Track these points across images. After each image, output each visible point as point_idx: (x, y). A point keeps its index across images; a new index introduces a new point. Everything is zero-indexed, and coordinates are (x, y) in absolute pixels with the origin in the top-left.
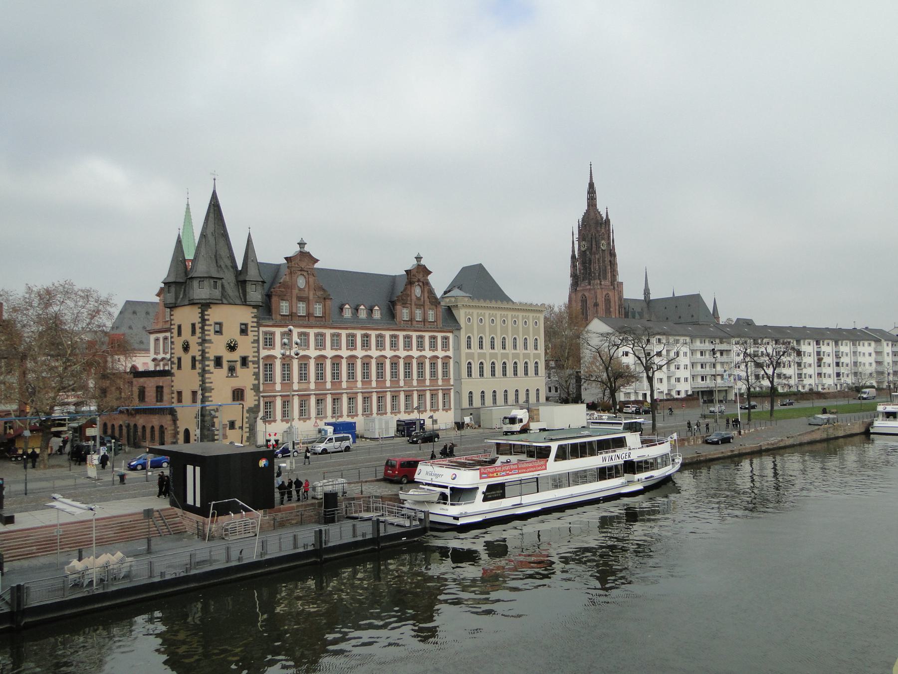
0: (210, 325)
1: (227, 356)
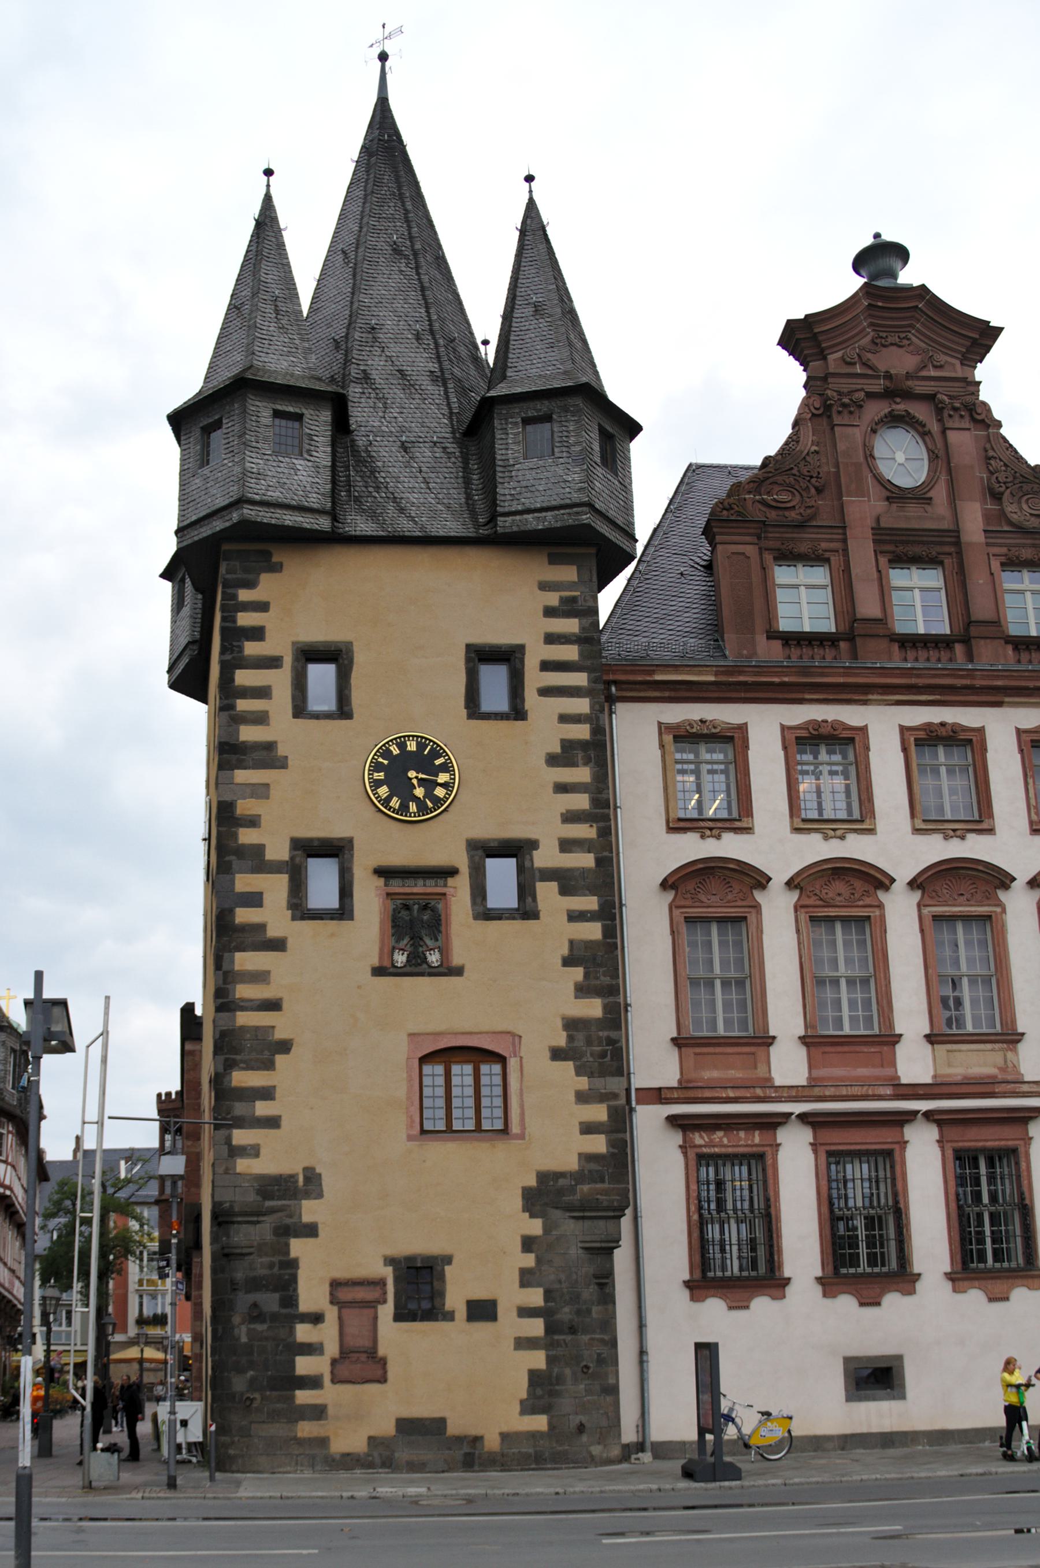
0: (273, 663)
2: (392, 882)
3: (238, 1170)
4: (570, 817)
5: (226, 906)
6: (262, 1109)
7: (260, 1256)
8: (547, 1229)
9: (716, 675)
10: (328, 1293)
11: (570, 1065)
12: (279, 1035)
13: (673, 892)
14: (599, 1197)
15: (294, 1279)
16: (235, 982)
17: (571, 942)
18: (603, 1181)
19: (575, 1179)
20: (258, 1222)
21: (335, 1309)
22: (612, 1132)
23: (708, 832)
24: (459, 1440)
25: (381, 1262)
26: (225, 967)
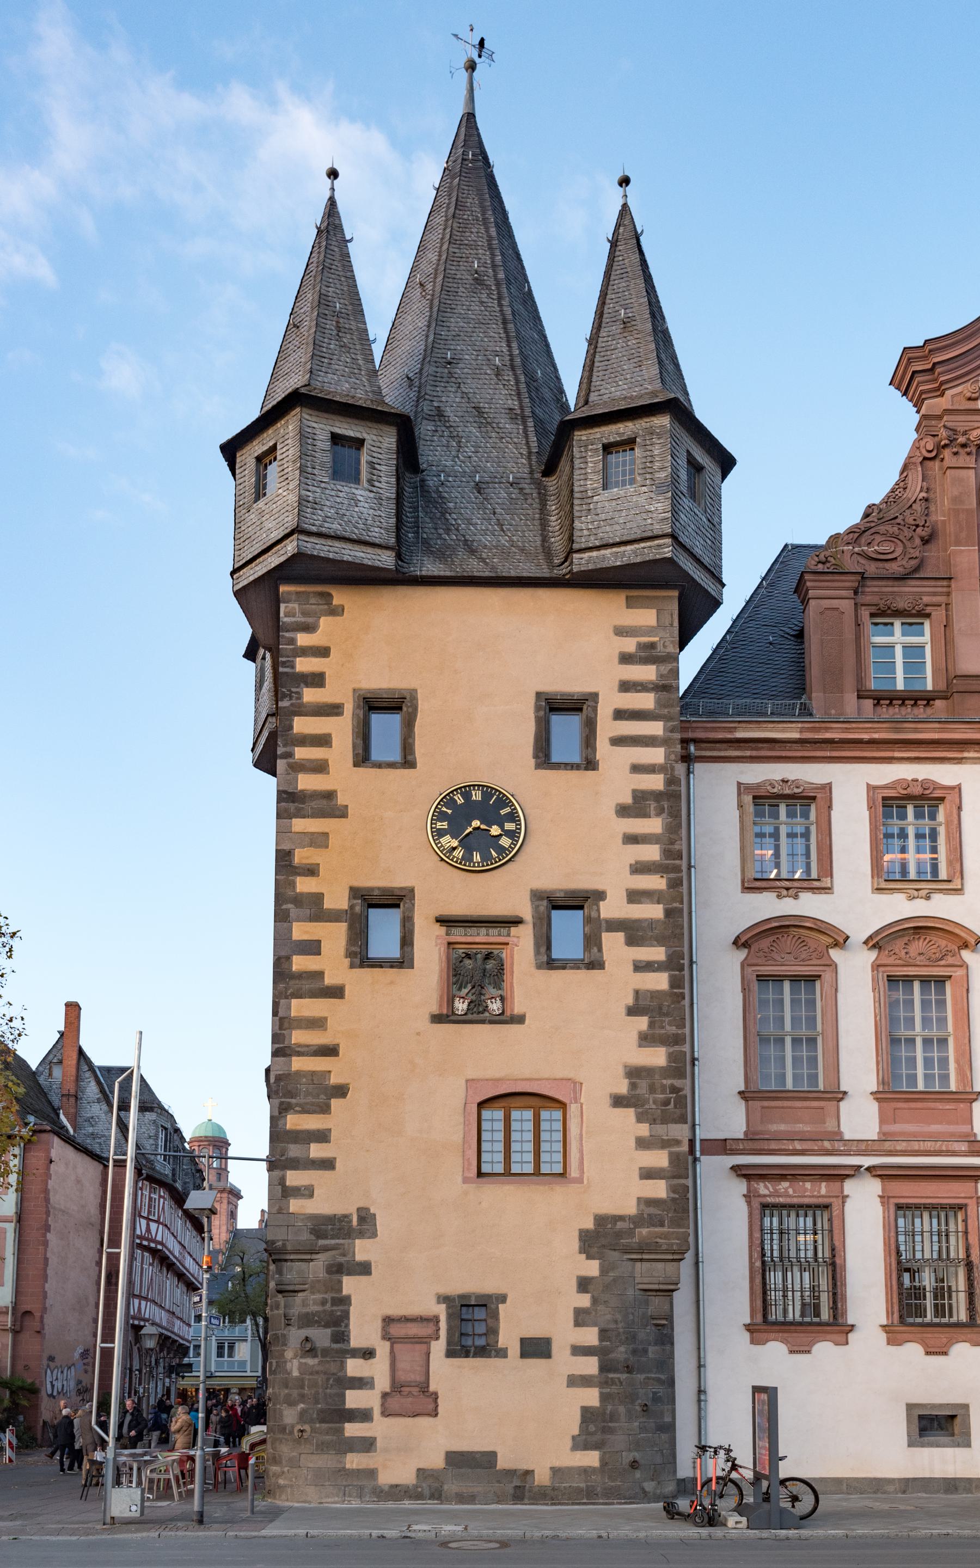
0: (334, 710)
1: (444, 889)
2: (454, 930)
3: (292, 1209)
4: (639, 868)
5: (283, 954)
6: (316, 1151)
7: (313, 1293)
8: (604, 1271)
9: (801, 731)
10: (380, 1330)
11: (630, 1113)
12: (334, 1080)
13: (746, 951)
14: (658, 1240)
15: (346, 1315)
16: (291, 1028)
17: (637, 992)
18: (662, 1225)
19: (634, 1223)
20: (312, 1260)
21: (388, 1344)
22: (674, 1177)
23: (785, 892)
24: (511, 1473)
25: (434, 1300)
26: (281, 1014)
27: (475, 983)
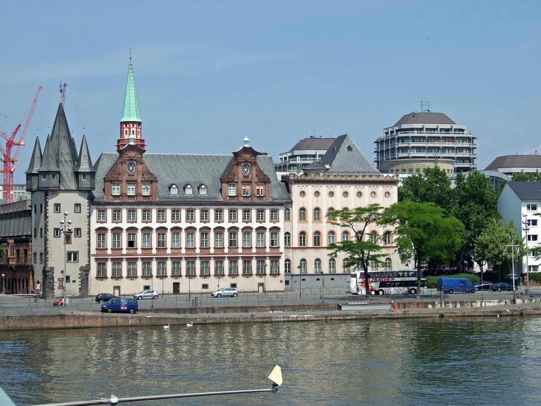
27: (68, 239)
